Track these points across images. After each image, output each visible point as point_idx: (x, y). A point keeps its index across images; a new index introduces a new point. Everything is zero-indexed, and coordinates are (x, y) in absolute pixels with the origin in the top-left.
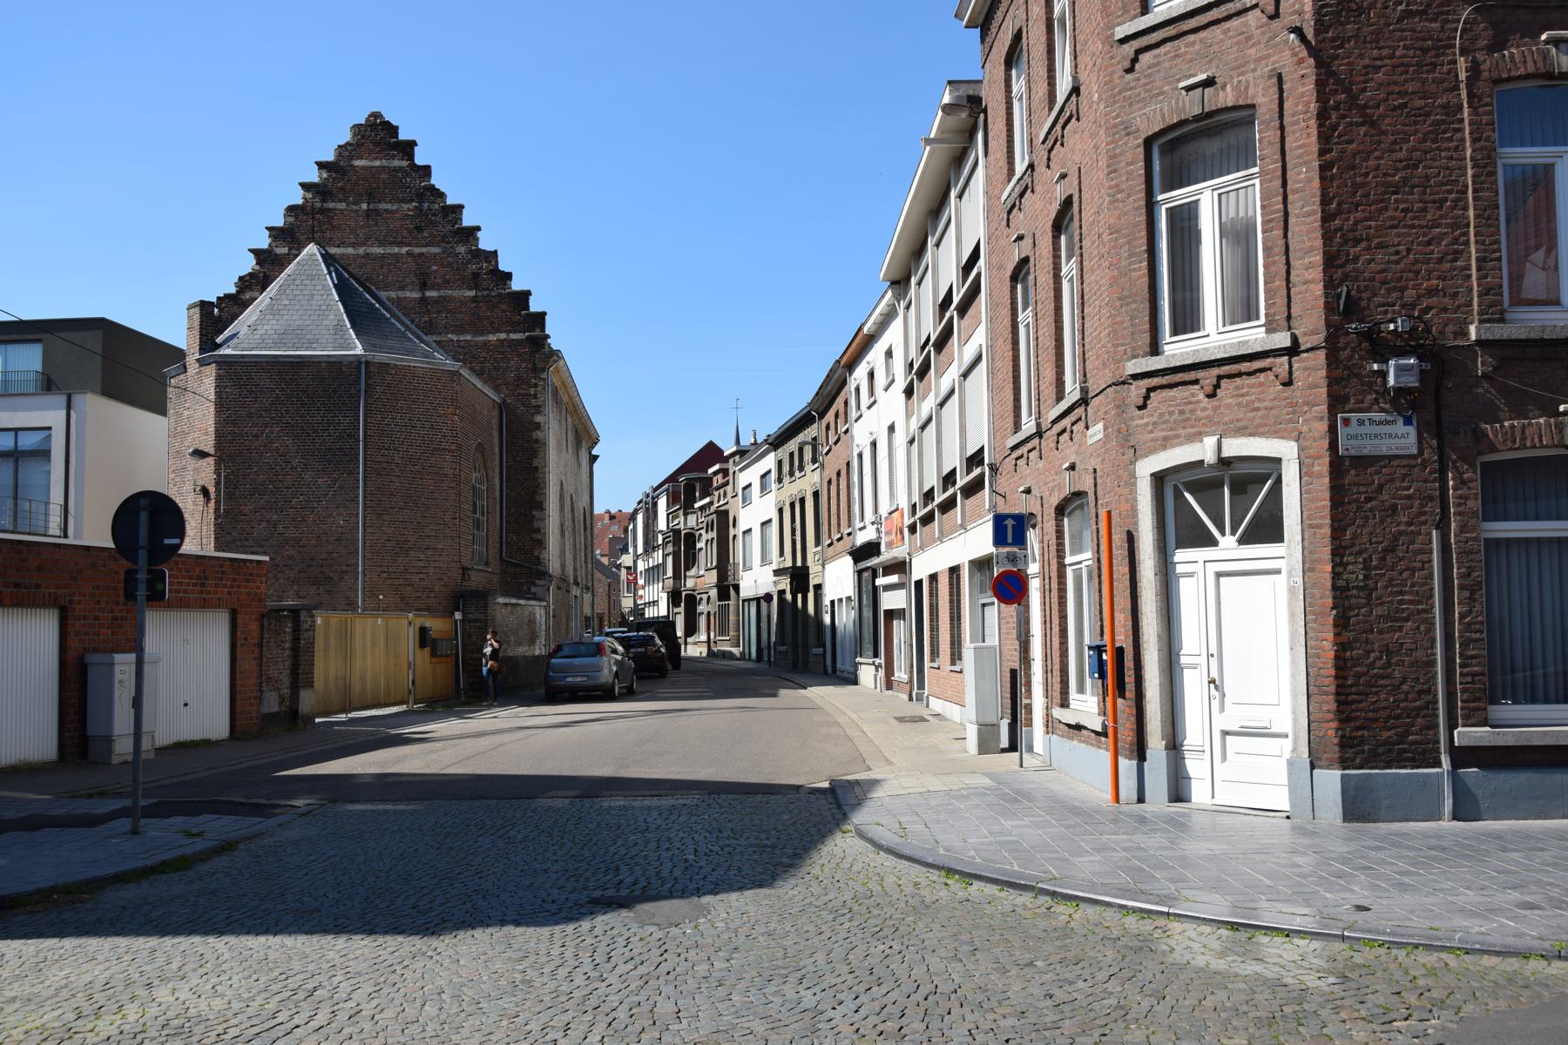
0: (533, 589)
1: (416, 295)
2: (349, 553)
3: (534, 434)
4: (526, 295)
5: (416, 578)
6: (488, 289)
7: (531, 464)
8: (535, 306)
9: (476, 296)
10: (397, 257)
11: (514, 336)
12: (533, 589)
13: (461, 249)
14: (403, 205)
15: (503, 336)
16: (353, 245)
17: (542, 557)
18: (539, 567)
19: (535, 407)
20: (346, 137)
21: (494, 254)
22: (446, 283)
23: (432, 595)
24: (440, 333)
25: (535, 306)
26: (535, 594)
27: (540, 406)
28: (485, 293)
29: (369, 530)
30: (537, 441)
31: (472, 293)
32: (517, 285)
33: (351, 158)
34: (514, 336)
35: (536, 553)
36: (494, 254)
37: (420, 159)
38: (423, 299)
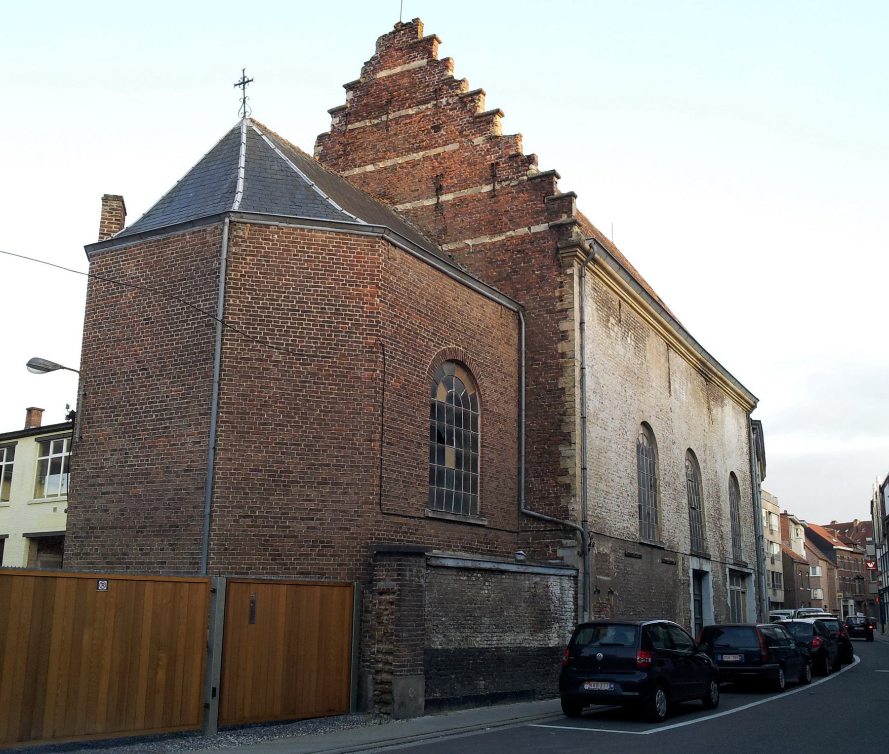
0: (560, 553)
1: (431, 202)
2: (197, 489)
3: (559, 346)
4: (551, 176)
5: (302, 527)
6: (507, 179)
7: (556, 385)
8: (562, 187)
9: (494, 190)
10: (414, 164)
11: (536, 229)
12: (560, 553)
13: (479, 140)
14: (421, 107)
15: (522, 231)
16: (373, 162)
17: (570, 507)
18: (567, 522)
19: (562, 311)
20: (370, 51)
21: (515, 138)
22: (465, 184)
23: (328, 552)
24: (456, 241)
25: (562, 187)
26: (562, 558)
27: (566, 310)
28: (504, 184)
29: (221, 455)
30: (563, 355)
31: (487, 188)
32: (542, 166)
33: (375, 71)
34: (536, 229)
35: (563, 502)
36: (515, 138)
37: (440, 53)
38: (438, 206)
